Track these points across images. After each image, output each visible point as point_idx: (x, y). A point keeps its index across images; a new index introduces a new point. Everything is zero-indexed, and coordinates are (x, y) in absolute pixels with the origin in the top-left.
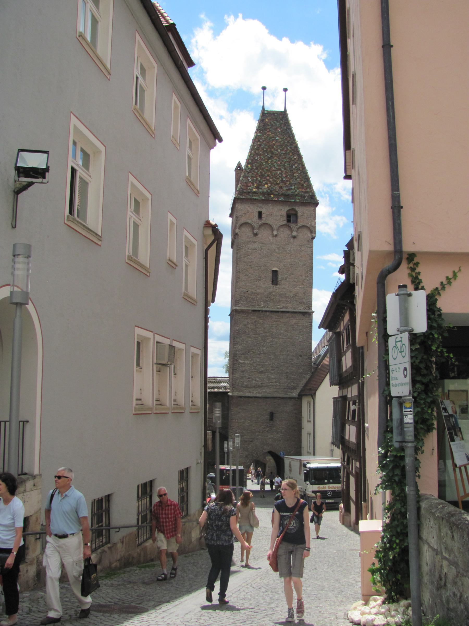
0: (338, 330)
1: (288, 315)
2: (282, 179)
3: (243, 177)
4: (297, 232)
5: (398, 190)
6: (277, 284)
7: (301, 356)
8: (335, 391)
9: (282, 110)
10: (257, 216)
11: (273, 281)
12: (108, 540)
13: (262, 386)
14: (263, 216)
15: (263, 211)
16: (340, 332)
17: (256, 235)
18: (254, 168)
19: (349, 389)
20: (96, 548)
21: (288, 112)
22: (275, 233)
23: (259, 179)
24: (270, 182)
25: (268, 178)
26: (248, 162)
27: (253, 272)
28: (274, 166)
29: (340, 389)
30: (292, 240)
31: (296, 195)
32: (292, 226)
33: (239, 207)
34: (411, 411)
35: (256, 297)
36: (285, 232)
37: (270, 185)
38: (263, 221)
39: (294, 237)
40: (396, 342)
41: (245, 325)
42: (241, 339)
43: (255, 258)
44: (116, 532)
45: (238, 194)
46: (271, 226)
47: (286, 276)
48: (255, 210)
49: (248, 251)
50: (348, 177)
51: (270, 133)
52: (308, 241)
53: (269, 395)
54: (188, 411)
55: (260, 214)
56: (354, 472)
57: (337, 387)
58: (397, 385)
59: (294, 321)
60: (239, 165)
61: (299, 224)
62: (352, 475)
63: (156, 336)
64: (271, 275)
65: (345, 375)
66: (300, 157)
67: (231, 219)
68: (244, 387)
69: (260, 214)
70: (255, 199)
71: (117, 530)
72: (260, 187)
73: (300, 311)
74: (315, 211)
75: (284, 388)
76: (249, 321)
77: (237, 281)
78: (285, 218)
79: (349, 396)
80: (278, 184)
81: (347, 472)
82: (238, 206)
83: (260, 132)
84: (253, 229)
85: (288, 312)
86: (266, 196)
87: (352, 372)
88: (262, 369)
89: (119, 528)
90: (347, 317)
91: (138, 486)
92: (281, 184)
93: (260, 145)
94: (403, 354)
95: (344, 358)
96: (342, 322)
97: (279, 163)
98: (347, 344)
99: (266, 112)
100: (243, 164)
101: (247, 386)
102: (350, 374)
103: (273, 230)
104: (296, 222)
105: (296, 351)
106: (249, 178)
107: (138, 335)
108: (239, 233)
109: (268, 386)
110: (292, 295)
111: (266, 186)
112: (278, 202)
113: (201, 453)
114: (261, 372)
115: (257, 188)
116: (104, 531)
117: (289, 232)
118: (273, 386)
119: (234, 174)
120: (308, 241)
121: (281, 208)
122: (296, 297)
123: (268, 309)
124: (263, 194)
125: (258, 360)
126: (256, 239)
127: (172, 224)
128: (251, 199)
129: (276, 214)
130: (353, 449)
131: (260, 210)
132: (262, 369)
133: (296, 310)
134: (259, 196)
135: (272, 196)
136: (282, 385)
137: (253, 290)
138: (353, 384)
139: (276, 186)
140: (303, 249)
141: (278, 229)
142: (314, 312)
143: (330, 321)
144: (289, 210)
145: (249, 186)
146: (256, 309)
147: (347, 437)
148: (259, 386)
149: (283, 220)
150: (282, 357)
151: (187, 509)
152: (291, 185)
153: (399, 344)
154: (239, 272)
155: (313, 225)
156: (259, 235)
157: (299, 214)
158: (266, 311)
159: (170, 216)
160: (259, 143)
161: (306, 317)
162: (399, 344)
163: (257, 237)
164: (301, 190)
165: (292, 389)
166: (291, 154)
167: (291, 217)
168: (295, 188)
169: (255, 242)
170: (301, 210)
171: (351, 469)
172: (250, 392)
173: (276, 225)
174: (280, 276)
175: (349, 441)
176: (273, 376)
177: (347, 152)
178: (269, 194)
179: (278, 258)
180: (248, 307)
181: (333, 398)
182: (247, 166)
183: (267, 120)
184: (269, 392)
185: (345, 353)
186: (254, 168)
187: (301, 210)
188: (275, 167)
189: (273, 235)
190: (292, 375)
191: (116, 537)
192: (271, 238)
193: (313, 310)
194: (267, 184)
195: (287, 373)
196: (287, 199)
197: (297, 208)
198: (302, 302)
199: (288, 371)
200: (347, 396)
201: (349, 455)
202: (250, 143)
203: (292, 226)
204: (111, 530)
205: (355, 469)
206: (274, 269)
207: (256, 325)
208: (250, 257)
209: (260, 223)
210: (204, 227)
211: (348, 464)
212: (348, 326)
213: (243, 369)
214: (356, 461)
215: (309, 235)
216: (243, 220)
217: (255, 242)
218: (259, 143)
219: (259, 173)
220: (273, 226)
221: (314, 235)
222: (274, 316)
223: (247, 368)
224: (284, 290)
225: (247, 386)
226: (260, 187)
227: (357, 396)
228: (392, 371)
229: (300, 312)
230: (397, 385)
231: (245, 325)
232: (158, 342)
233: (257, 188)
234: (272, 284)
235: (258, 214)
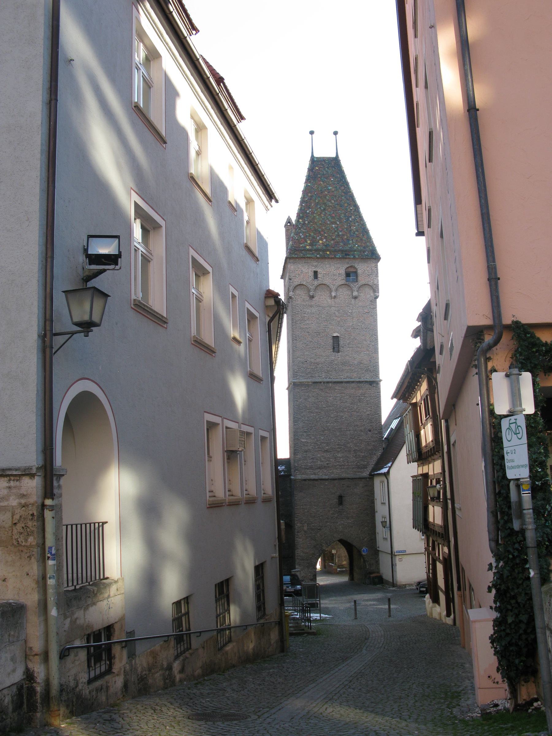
0: (414, 401)
1: (353, 384)
2: (338, 233)
3: (295, 234)
4: (358, 291)
5: (494, 261)
6: (339, 352)
7: (370, 431)
8: (414, 469)
9: (334, 156)
10: (312, 277)
11: (334, 348)
12: (189, 647)
13: (328, 467)
14: (319, 276)
15: (319, 270)
16: (416, 402)
17: (312, 297)
18: (306, 222)
19: (431, 465)
20: (178, 654)
21: (341, 158)
22: (333, 294)
23: (312, 234)
24: (326, 237)
25: (322, 233)
26: (299, 216)
27: (311, 339)
28: (328, 219)
29: (418, 466)
31: (355, 251)
32: (352, 285)
33: (292, 267)
34: (529, 493)
35: (317, 367)
36: (344, 293)
37: (325, 240)
38: (320, 282)
39: (356, 298)
40: (510, 424)
41: (305, 399)
42: (302, 415)
44: (197, 636)
45: (290, 253)
46: (328, 286)
47: (348, 341)
50: (420, 233)
51: (322, 183)
52: (371, 301)
53: (337, 476)
54: (259, 501)
55: (316, 273)
56: (441, 558)
57: (416, 464)
58: (513, 467)
59: (360, 391)
60: (289, 221)
62: (439, 562)
63: (225, 420)
64: (332, 341)
65: (424, 450)
66: (357, 208)
67: (283, 280)
68: (308, 469)
69: (316, 273)
70: (310, 258)
71: (198, 634)
72: (314, 244)
73: (366, 380)
74: (376, 267)
75: (353, 468)
76: (310, 395)
77: (293, 351)
78: (344, 276)
79: (431, 473)
80: (333, 239)
81: (433, 558)
82: (291, 267)
83: (310, 182)
84: (309, 291)
85: (353, 382)
86: (321, 253)
87: (434, 447)
88: (327, 447)
89: (200, 632)
90: (424, 386)
91: (216, 585)
92: (337, 239)
93: (312, 197)
94: (519, 436)
95: (422, 432)
96: (419, 392)
97: (334, 215)
98: (426, 416)
99: (315, 159)
100: (294, 219)
101: (311, 468)
102: (431, 449)
103: (331, 291)
104: (357, 281)
105: (364, 425)
106: (301, 234)
107: (207, 421)
108: (293, 297)
109: (336, 466)
110: (356, 362)
111: (321, 242)
112: (335, 258)
113: (275, 545)
114: (327, 451)
115: (311, 244)
116: (185, 636)
117: (350, 293)
118: (340, 466)
119: (283, 230)
120: (371, 301)
121: (338, 265)
122: (361, 365)
123: (330, 380)
124: (317, 250)
125: (322, 438)
127: (234, 296)
128: (304, 258)
129: (332, 271)
130: (439, 533)
131: (315, 270)
132: (327, 447)
133: (362, 380)
134: (312, 254)
135: (328, 253)
136: (350, 464)
137: (312, 360)
138: (434, 460)
139: (332, 242)
141: (336, 290)
142: (380, 381)
143: (404, 391)
144: (348, 268)
145: (301, 244)
146: (317, 380)
147: (431, 519)
148: (325, 467)
149: (341, 280)
150: (348, 432)
151: (264, 609)
152: (349, 240)
153: (513, 426)
154: (296, 340)
155: (375, 283)
157: (359, 272)
158: (328, 382)
159: (232, 290)
160: (309, 195)
161: (374, 387)
162: (513, 426)
163: (314, 299)
164: (359, 244)
165: (362, 468)
166: (346, 205)
167: (351, 275)
168: (353, 242)
169: (311, 306)
170: (362, 268)
171: (437, 555)
172: (315, 474)
173: (334, 285)
174: (341, 342)
175: (434, 524)
176: (339, 455)
177: (418, 206)
178: (324, 251)
180: (307, 378)
181: (412, 477)
182: (297, 221)
183: (317, 168)
184: (336, 473)
185: (424, 425)
186: (306, 222)
187: (362, 268)
188: (329, 221)
190: (362, 452)
191: (195, 642)
193: (381, 378)
194: (321, 239)
195: (355, 450)
196: (346, 255)
198: (367, 370)
199: (357, 448)
200: (428, 473)
201: (435, 539)
202: (300, 195)
203: (352, 285)
204: (192, 635)
205: (443, 554)
206: (335, 335)
207: (318, 399)
208: (307, 322)
209: (316, 283)
210: (265, 297)
211: (434, 549)
212: (427, 396)
213: (306, 448)
214: (443, 545)
215: (372, 294)
216: (297, 282)
217: (311, 306)
218: (309, 195)
219: (312, 228)
220: (331, 286)
221: (377, 294)
222: (337, 387)
223: (310, 448)
224: (347, 358)
225: (311, 468)
226: (314, 244)
227: (441, 473)
228: (507, 453)
229: (366, 382)
230: (513, 467)
231: (305, 399)
232: (227, 428)
233: (311, 244)
234: (333, 352)
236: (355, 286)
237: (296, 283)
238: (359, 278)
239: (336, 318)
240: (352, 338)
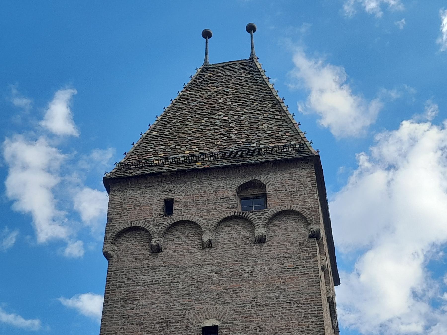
14: (175, 207)
15: (176, 197)
17: (156, 250)
22: (206, 238)
30: (256, 249)
32: (251, 216)
36: (233, 235)
38: (175, 218)
39: (261, 241)
43: (153, 304)
48: (157, 197)
49: (134, 292)
61: (272, 210)
121: (221, 183)
126: (157, 261)
131: (167, 196)
140: (288, 264)
156: (165, 252)
157: (269, 189)
169: (154, 268)
179: (220, 295)
189: (202, 244)
192: (199, 254)
197: (263, 179)
206: (208, 323)
208: (141, 302)
209: (168, 221)
217: (154, 268)
220: (203, 222)
235: (163, 204)
236: (259, 219)
237: (122, 226)
238: (270, 200)
239: (213, 287)
240: (253, 326)
